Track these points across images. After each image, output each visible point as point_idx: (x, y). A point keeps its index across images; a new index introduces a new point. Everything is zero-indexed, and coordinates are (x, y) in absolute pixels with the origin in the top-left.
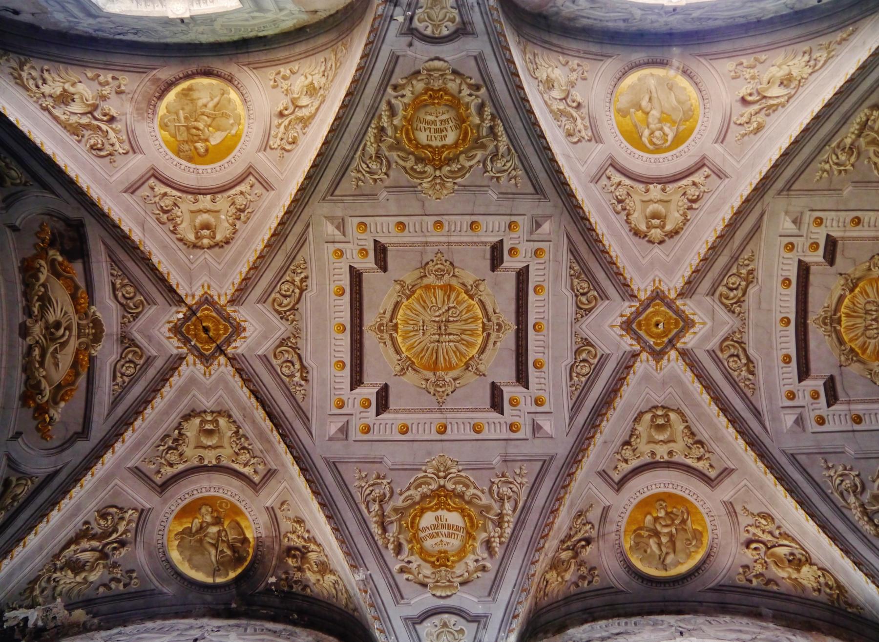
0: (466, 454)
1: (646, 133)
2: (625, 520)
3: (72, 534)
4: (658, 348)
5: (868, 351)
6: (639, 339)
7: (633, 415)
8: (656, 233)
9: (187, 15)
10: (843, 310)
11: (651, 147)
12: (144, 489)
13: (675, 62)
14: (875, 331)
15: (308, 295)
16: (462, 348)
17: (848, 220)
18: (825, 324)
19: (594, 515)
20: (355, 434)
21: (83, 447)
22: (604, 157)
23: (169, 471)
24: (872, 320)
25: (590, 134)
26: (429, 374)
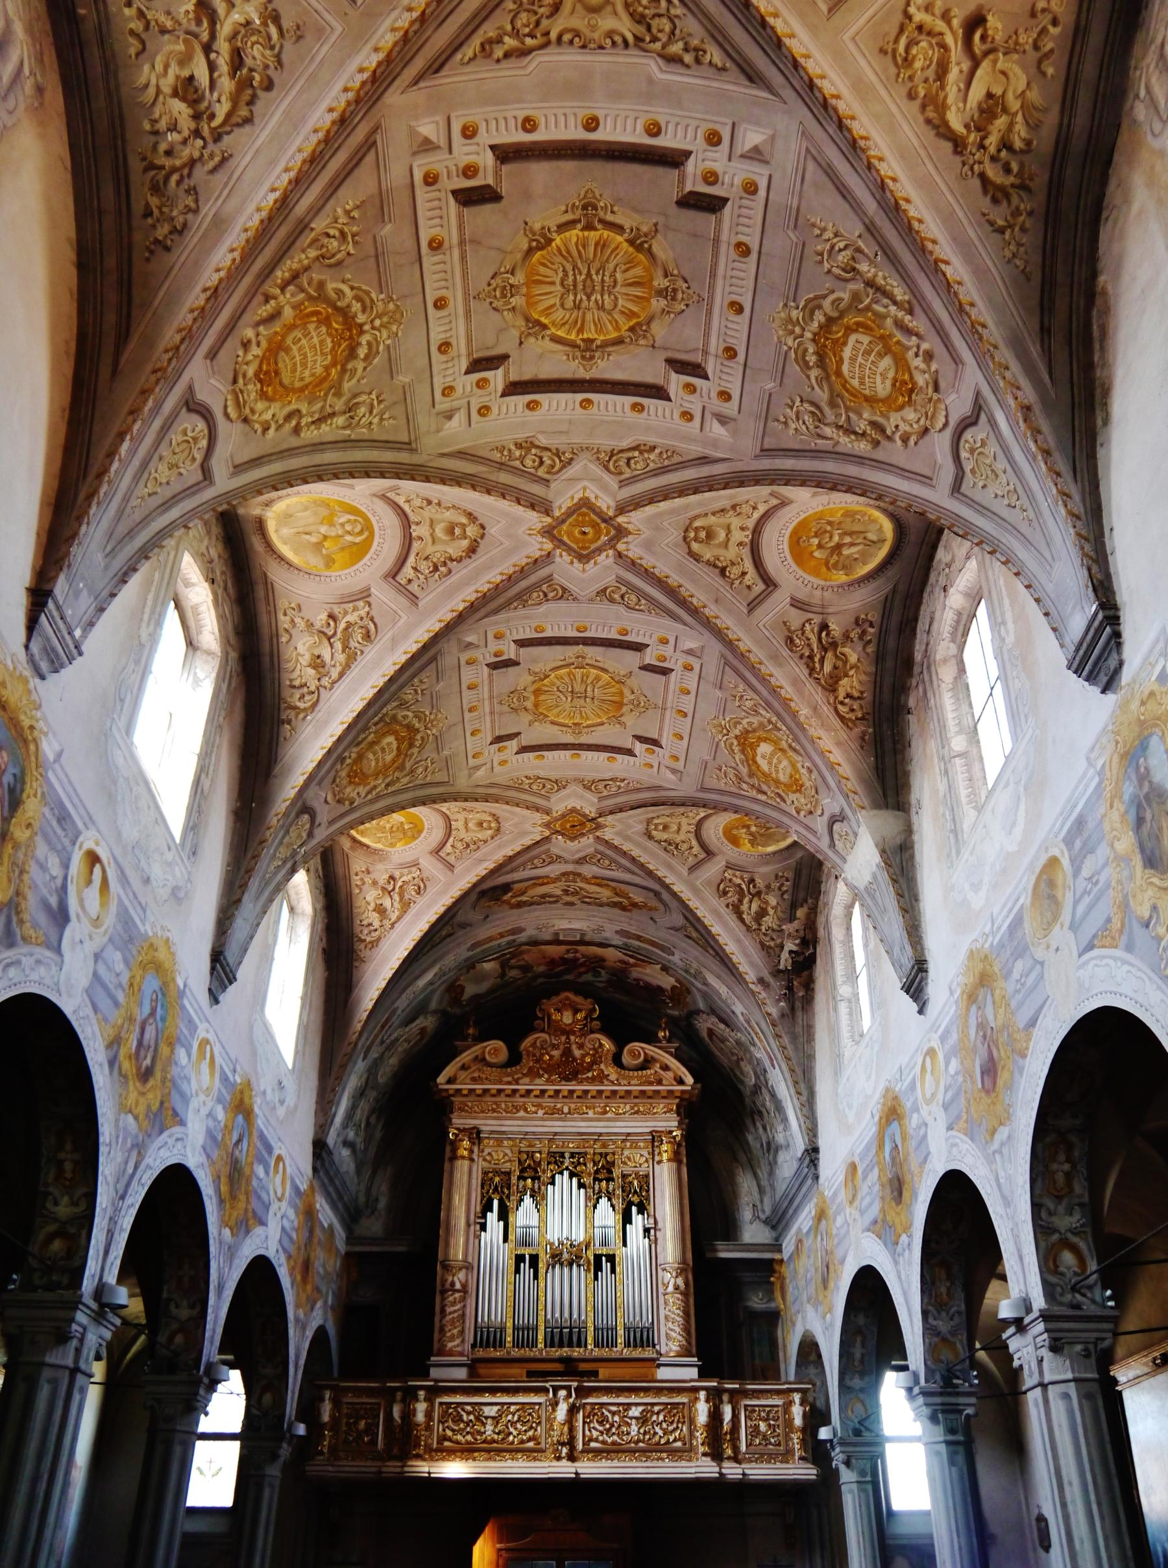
0: (707, 710)
1: (349, 538)
2: (812, 579)
3: (734, 917)
4: (613, 532)
5: (635, 309)
6: (599, 550)
7: (691, 564)
8: (472, 531)
9: (206, 585)
10: (573, 337)
11: (366, 534)
12: (708, 865)
13: (257, 511)
14: (606, 297)
15: (542, 774)
16: (600, 684)
17: (443, 358)
18: (592, 358)
19: (796, 618)
20: (680, 765)
21: (665, 896)
22: (385, 586)
23: (696, 849)
24: (589, 299)
25: (361, 604)
26: (625, 709)
